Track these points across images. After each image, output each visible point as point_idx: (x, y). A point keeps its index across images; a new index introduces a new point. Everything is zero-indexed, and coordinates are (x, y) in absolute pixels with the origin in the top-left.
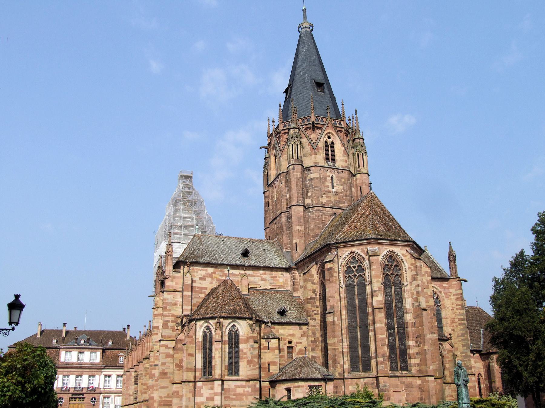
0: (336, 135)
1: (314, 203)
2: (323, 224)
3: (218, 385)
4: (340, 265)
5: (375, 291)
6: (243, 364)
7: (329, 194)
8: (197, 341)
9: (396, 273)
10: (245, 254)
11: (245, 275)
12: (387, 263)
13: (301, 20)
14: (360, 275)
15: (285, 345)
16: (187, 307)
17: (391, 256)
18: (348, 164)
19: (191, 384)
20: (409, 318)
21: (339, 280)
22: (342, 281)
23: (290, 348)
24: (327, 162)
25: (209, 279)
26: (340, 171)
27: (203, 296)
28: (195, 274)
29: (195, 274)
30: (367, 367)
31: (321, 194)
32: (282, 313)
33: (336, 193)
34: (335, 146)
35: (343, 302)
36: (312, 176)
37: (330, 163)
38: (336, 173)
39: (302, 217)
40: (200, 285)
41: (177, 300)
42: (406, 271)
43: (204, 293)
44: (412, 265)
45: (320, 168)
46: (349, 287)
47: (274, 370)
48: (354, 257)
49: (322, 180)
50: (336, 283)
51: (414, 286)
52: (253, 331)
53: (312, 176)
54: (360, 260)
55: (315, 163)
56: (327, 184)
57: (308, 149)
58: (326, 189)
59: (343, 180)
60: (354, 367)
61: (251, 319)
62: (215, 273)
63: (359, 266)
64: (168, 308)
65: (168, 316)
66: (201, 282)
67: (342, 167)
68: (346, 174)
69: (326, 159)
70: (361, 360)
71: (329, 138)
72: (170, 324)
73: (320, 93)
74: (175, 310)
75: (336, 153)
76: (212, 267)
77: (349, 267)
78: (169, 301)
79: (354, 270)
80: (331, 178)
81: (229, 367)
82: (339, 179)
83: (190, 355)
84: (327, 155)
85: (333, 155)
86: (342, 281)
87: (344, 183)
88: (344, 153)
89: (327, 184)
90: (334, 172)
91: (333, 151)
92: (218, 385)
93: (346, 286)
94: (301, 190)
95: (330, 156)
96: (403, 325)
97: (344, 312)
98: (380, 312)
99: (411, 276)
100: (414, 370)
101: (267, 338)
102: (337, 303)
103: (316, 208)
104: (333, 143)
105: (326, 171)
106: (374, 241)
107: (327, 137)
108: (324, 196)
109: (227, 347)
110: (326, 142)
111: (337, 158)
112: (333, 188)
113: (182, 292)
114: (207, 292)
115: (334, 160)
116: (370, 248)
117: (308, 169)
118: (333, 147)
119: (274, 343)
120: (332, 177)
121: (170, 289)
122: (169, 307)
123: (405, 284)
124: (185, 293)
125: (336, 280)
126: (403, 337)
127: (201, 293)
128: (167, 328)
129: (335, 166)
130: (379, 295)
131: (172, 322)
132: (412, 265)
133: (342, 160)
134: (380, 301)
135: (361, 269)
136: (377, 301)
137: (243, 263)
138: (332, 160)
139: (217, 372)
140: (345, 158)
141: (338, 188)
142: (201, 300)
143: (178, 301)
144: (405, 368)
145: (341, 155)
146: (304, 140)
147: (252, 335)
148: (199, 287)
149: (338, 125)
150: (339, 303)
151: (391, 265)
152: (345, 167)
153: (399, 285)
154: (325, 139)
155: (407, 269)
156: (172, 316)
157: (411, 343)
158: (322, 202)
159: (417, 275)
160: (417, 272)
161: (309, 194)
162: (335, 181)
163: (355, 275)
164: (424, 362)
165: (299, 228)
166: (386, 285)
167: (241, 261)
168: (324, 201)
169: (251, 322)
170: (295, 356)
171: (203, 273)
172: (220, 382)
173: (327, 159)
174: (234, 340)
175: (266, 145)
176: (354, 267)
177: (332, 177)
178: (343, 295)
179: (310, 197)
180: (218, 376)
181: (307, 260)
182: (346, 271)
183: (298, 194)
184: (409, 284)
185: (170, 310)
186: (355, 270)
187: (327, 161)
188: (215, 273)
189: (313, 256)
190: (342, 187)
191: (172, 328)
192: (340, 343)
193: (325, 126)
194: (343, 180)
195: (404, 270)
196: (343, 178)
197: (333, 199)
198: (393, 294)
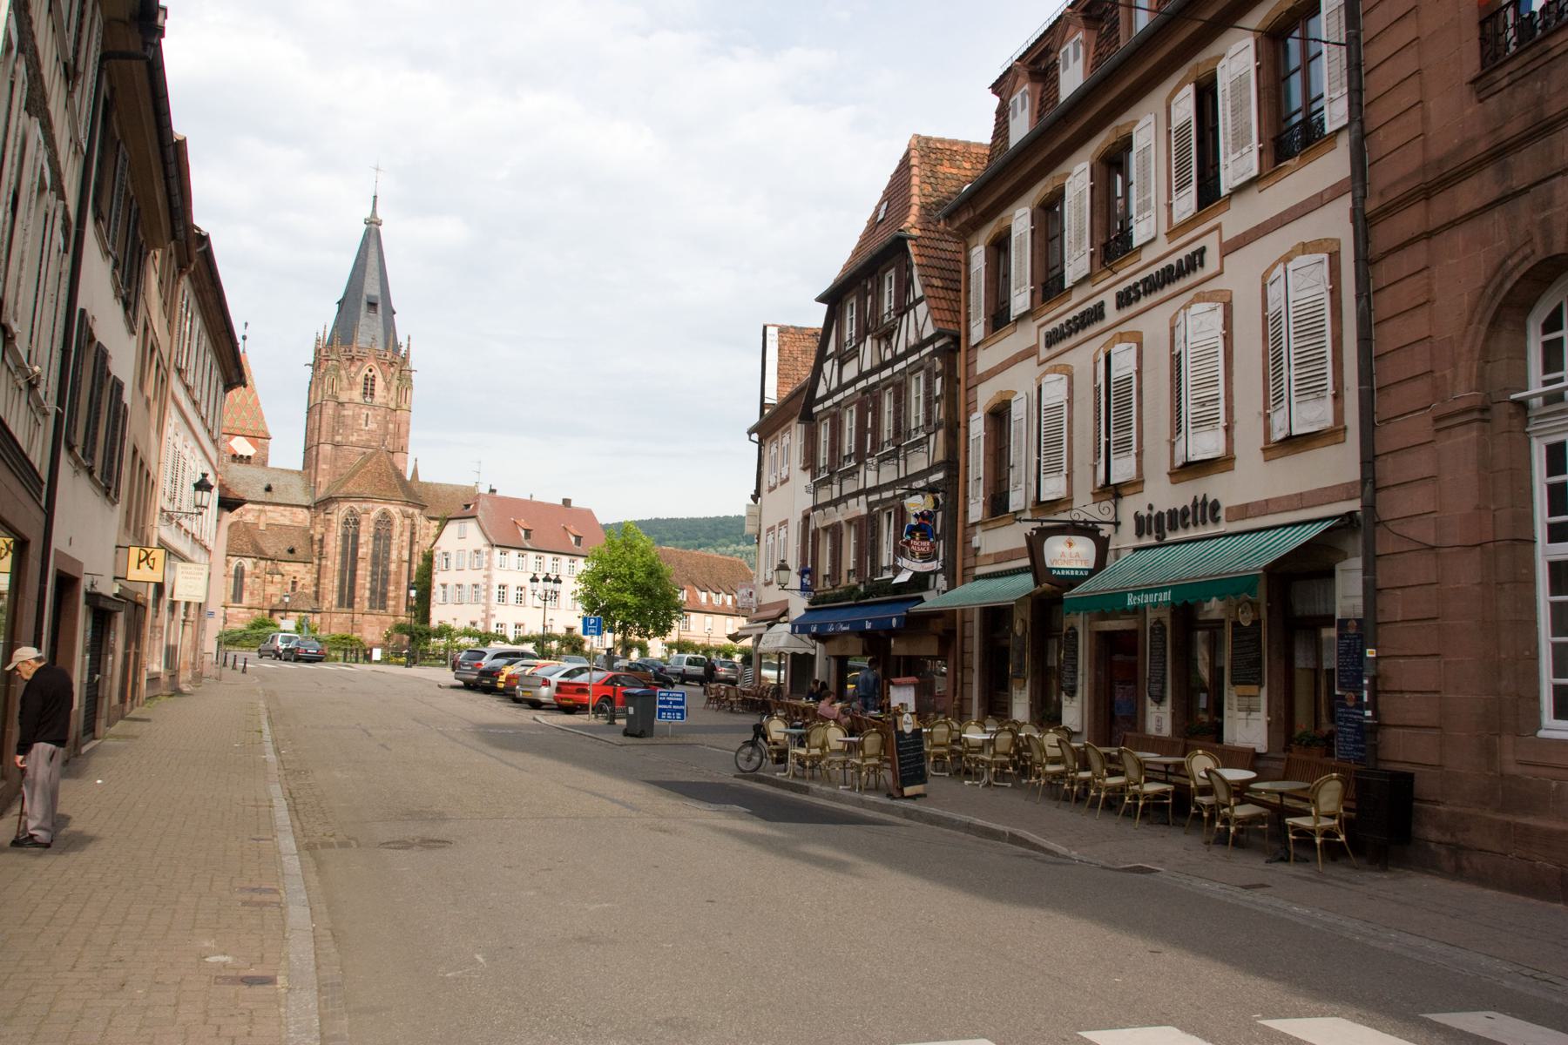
6: (246, 595)
13: (368, 215)
15: (289, 580)
17: (385, 514)
20: (393, 567)
23: (294, 583)
30: (351, 605)
32: (292, 551)
33: (369, 432)
35: (339, 549)
37: (368, 399)
46: (345, 536)
47: (275, 600)
48: (352, 512)
49: (355, 417)
54: (358, 514)
57: (345, 381)
60: (341, 604)
68: (382, 412)
70: (347, 598)
81: (234, 597)
82: (375, 416)
96: (386, 573)
97: (338, 558)
100: (390, 610)
101: (272, 574)
106: (365, 499)
115: (372, 395)
116: (364, 505)
117: (342, 404)
119: (277, 578)
126: (385, 582)
135: (357, 523)
141: (372, 426)
144: (384, 607)
146: (343, 372)
153: (390, 538)
157: (392, 588)
164: (396, 606)
166: (377, 537)
167: (262, 496)
170: (298, 589)
186: (353, 522)
192: (331, 584)
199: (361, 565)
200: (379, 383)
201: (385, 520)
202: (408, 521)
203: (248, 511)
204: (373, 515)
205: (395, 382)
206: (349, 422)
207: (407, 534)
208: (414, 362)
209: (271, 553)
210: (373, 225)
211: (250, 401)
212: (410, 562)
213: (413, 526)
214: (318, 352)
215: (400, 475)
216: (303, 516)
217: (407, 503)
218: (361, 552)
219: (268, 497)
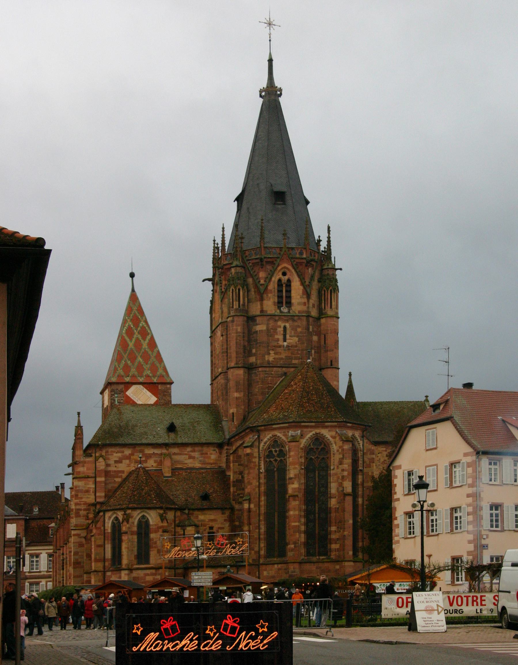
0: (293, 271)
1: (259, 362)
2: (269, 388)
3: (125, 574)
4: (261, 449)
5: (290, 479)
7: (279, 350)
8: (106, 531)
9: (322, 457)
10: (172, 428)
11: (169, 455)
12: (312, 447)
14: (281, 460)
16: (101, 494)
17: (318, 439)
18: (308, 307)
19: (100, 574)
21: (259, 466)
22: (262, 466)
24: (279, 308)
25: (127, 461)
26: (296, 318)
27: (118, 480)
28: (110, 457)
29: (110, 457)
31: (268, 350)
34: (292, 284)
35: (263, 489)
36: (258, 328)
37: (285, 310)
38: (291, 322)
39: (241, 382)
40: (115, 469)
41: (89, 486)
42: (334, 454)
43: (121, 477)
44: (340, 447)
45: (270, 317)
46: (269, 472)
49: (270, 332)
50: (254, 468)
51: (340, 470)
52: (162, 521)
53: (258, 328)
55: (262, 311)
56: (276, 337)
58: (275, 344)
59: (299, 330)
61: (161, 508)
62: (132, 454)
63: (281, 451)
64: (79, 496)
65: (80, 504)
66: (116, 465)
67: (299, 312)
69: (278, 303)
71: (284, 274)
72: (82, 513)
73: (279, 206)
74: (88, 498)
75: (293, 294)
76: (129, 448)
77: (271, 451)
78: (80, 488)
79: (276, 454)
80: (282, 329)
82: (294, 328)
83: (99, 546)
84: (280, 297)
85: (289, 297)
86: (262, 466)
87: (301, 332)
88: (303, 294)
89: (276, 337)
90: (287, 321)
91: (289, 291)
92: (125, 574)
93: (267, 471)
94: (242, 347)
95: (284, 298)
98: (295, 500)
99: (338, 459)
102: (254, 490)
103: (260, 369)
104: (289, 281)
105: (276, 321)
107: (280, 273)
108: (272, 352)
109: (135, 537)
110: (280, 280)
111: (293, 301)
112: (285, 340)
113: (95, 477)
114: (124, 476)
115: (289, 304)
118: (290, 286)
120: (285, 328)
121: (81, 475)
122: (80, 495)
123: (332, 468)
124: (98, 479)
125: (256, 466)
127: (118, 477)
128: (80, 516)
129: (289, 312)
130: (296, 482)
131: (85, 510)
132: (340, 447)
133: (299, 304)
134: (295, 488)
136: (294, 489)
137: (167, 441)
138: (286, 303)
139: (125, 561)
140: (305, 300)
141: (292, 340)
142: (116, 485)
143: (91, 488)
145: (299, 297)
147: (162, 524)
148: (115, 471)
149: (298, 256)
150: (257, 490)
151: (317, 449)
152: (303, 312)
154: (278, 278)
155: (335, 452)
156: (84, 504)
158: (268, 361)
159: (343, 458)
160: (343, 456)
161: (254, 351)
162: (288, 332)
163: (276, 460)
165: (236, 395)
168: (271, 359)
169: (162, 512)
171: (119, 455)
172: (127, 572)
173: (279, 304)
174: (144, 529)
175: (211, 277)
176: (276, 451)
177: (285, 328)
178: (262, 481)
179: (255, 355)
180: (125, 565)
181: (237, 437)
182: (268, 456)
183: (237, 352)
184: (336, 467)
185: (82, 498)
187: (280, 305)
188: (132, 454)
189: (241, 435)
190: (296, 339)
191: (84, 516)
193: (278, 260)
194: (299, 330)
195: (332, 452)
196: (299, 327)
197: (283, 356)
198: (317, 479)
199: (294, 504)
200: (297, 287)
201: (320, 447)
202: (347, 446)
203: (149, 456)
204: (303, 442)
205: (315, 285)
206: (263, 338)
207: (348, 461)
208: (339, 257)
209: (181, 500)
210: (271, 96)
211: (145, 344)
212: (354, 494)
213: (355, 451)
214: (216, 261)
215: (334, 392)
216: (213, 455)
217: (342, 425)
218: (293, 487)
219: (171, 438)
